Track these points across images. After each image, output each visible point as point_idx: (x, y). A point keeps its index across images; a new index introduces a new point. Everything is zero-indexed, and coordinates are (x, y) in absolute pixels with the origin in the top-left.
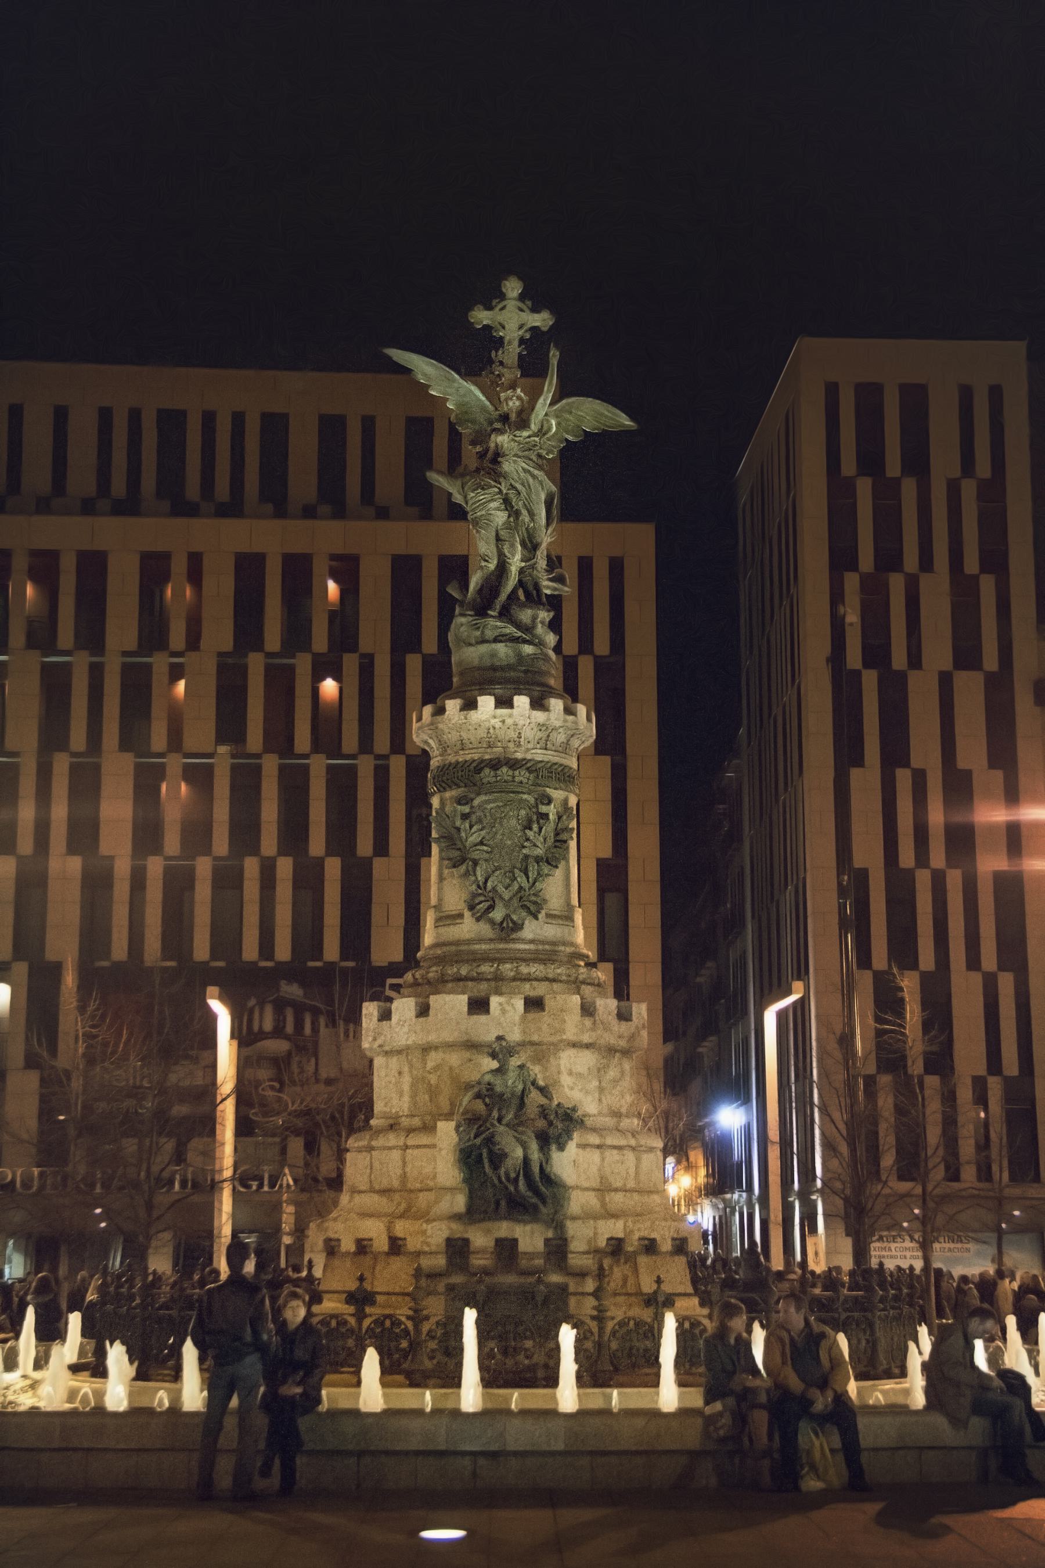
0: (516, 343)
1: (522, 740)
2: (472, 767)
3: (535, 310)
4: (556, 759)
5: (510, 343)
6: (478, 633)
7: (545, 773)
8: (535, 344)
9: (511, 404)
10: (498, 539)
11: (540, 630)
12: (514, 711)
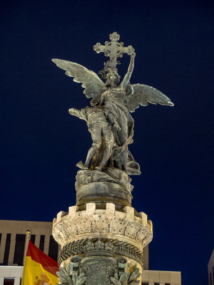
0: (116, 59)
1: (111, 229)
2: (82, 243)
3: (125, 45)
4: (130, 242)
5: (113, 58)
6: (90, 178)
7: (123, 248)
8: (124, 61)
9: (111, 77)
10: (102, 135)
11: (123, 181)
12: (106, 210)
